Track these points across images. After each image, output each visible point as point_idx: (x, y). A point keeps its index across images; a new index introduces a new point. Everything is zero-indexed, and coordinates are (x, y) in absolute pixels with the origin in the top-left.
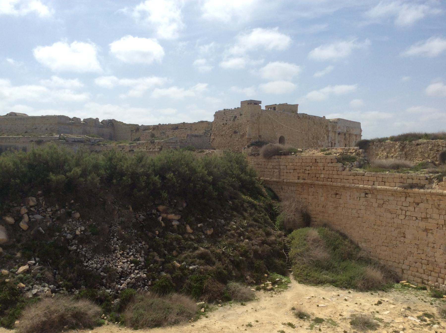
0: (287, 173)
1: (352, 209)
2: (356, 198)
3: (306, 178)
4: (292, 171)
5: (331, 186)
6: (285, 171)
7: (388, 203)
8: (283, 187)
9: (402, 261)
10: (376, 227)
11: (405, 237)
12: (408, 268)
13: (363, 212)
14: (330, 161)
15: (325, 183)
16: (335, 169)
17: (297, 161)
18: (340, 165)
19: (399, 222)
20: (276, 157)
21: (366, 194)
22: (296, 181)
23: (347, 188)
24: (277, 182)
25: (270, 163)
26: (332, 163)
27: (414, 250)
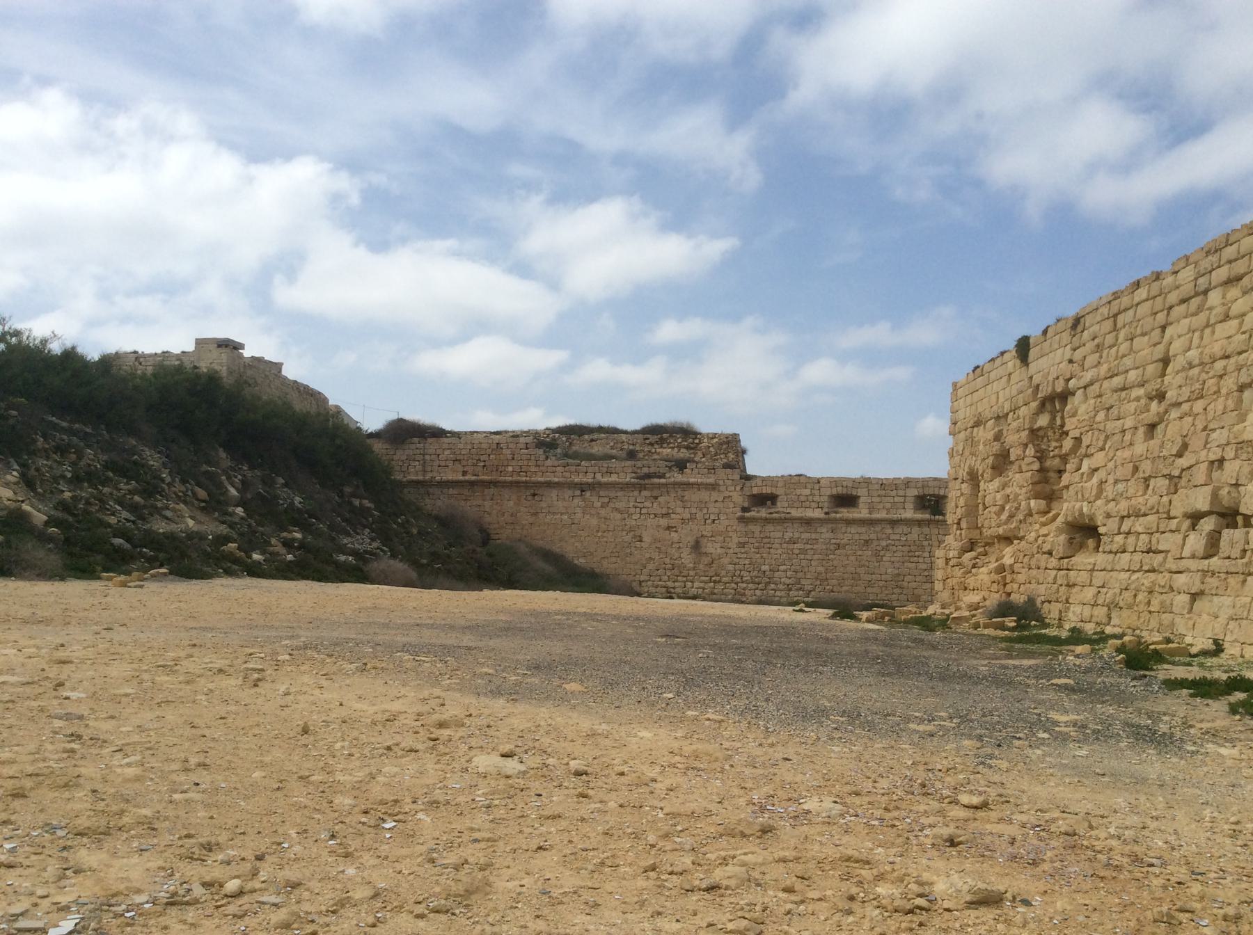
0: (439, 466)
1: (562, 514)
2: (567, 498)
3: (480, 474)
4: (450, 464)
5: (526, 482)
6: (436, 463)
7: (614, 500)
8: (431, 490)
9: (639, 572)
10: (599, 534)
11: (641, 541)
12: (647, 578)
13: (579, 516)
14: (524, 446)
15: (515, 478)
16: (533, 458)
17: (461, 446)
18: (541, 452)
19: (634, 523)
20: (416, 440)
21: (582, 491)
22: (461, 478)
23: (556, 483)
24: (418, 482)
25: (399, 452)
26: (527, 449)
27: (656, 555)
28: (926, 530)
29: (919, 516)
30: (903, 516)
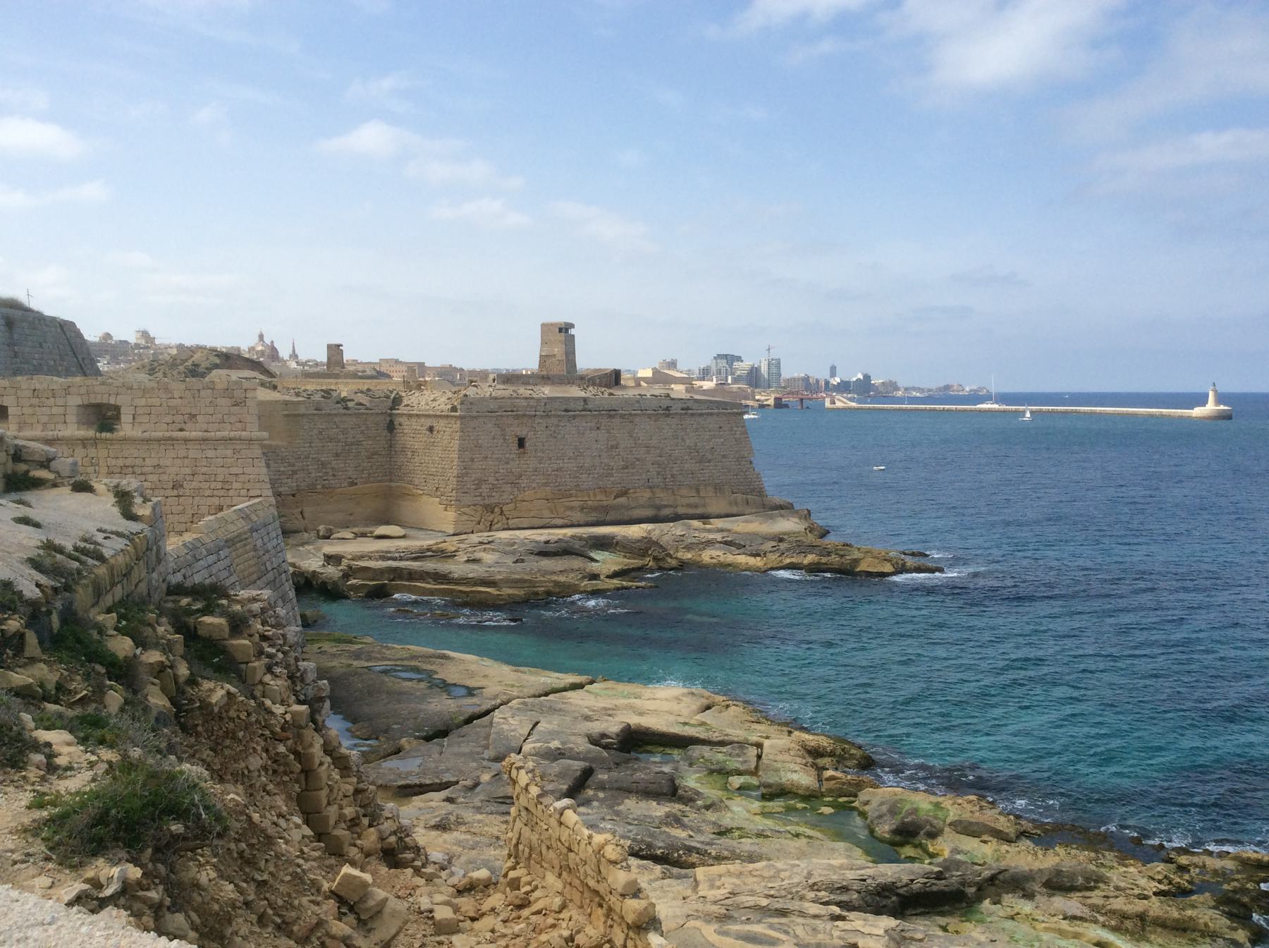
28: (92, 452)
29: (82, 433)
30: (60, 434)
